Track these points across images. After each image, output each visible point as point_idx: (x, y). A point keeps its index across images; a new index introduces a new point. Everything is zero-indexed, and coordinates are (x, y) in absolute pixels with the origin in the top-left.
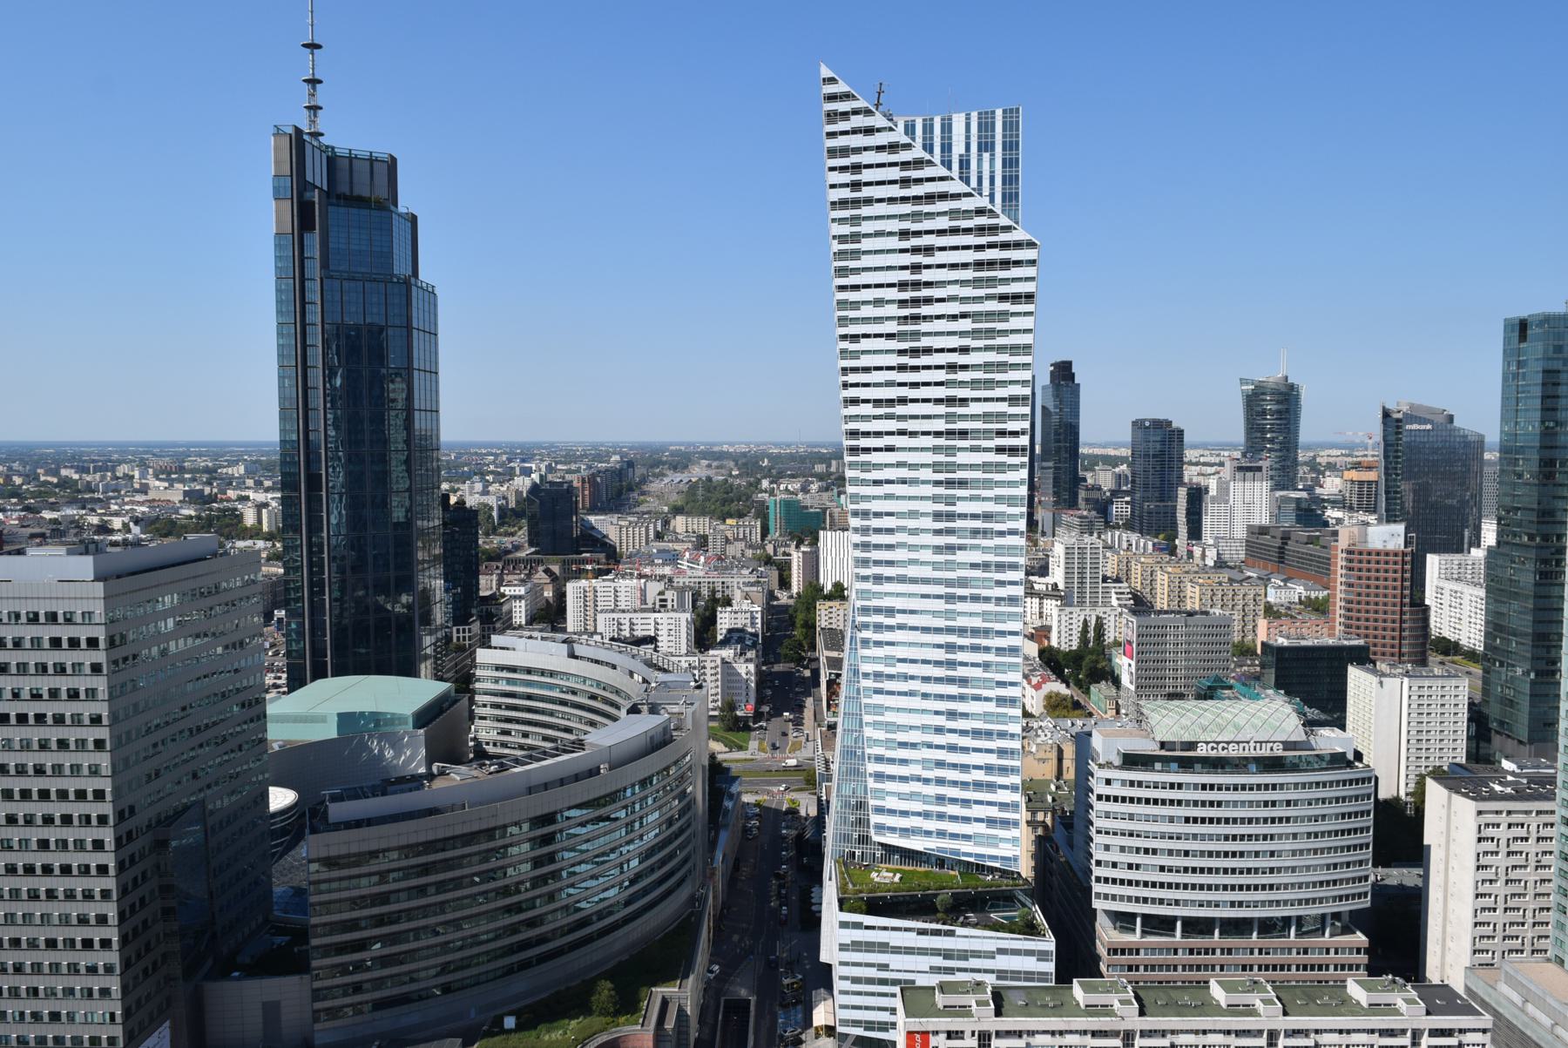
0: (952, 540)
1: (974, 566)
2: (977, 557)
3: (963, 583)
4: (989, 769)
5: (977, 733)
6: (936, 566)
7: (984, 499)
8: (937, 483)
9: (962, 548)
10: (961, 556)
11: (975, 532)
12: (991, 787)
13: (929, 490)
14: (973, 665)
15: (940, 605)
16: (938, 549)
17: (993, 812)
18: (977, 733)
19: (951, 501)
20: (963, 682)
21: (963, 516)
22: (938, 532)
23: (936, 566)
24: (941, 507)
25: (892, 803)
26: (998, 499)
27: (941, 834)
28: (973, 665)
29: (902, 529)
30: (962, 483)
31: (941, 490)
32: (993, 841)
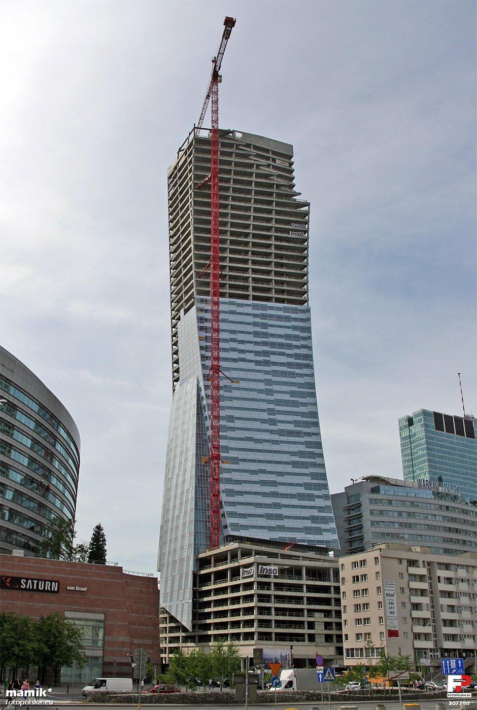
0: (267, 348)
1: (282, 364)
2: (283, 359)
3: (275, 373)
4: (307, 486)
5: (295, 464)
6: (258, 363)
7: (286, 327)
8: (255, 316)
9: (274, 353)
10: (273, 358)
11: (281, 345)
12: (311, 497)
13: (250, 319)
14: (288, 422)
15: (262, 386)
16: (257, 353)
17: (315, 513)
18: (295, 464)
19: (265, 326)
20: (281, 432)
21: (273, 335)
22: (256, 343)
23: (258, 363)
24: (258, 329)
25: (240, 509)
26: (295, 328)
27: (281, 528)
28: (288, 422)
29: (234, 340)
30: (271, 317)
31: (258, 320)
32: (319, 531)
